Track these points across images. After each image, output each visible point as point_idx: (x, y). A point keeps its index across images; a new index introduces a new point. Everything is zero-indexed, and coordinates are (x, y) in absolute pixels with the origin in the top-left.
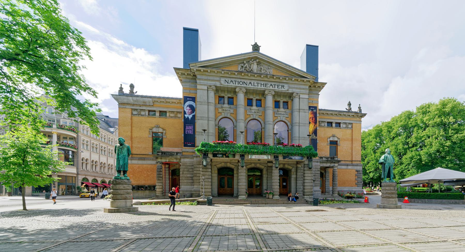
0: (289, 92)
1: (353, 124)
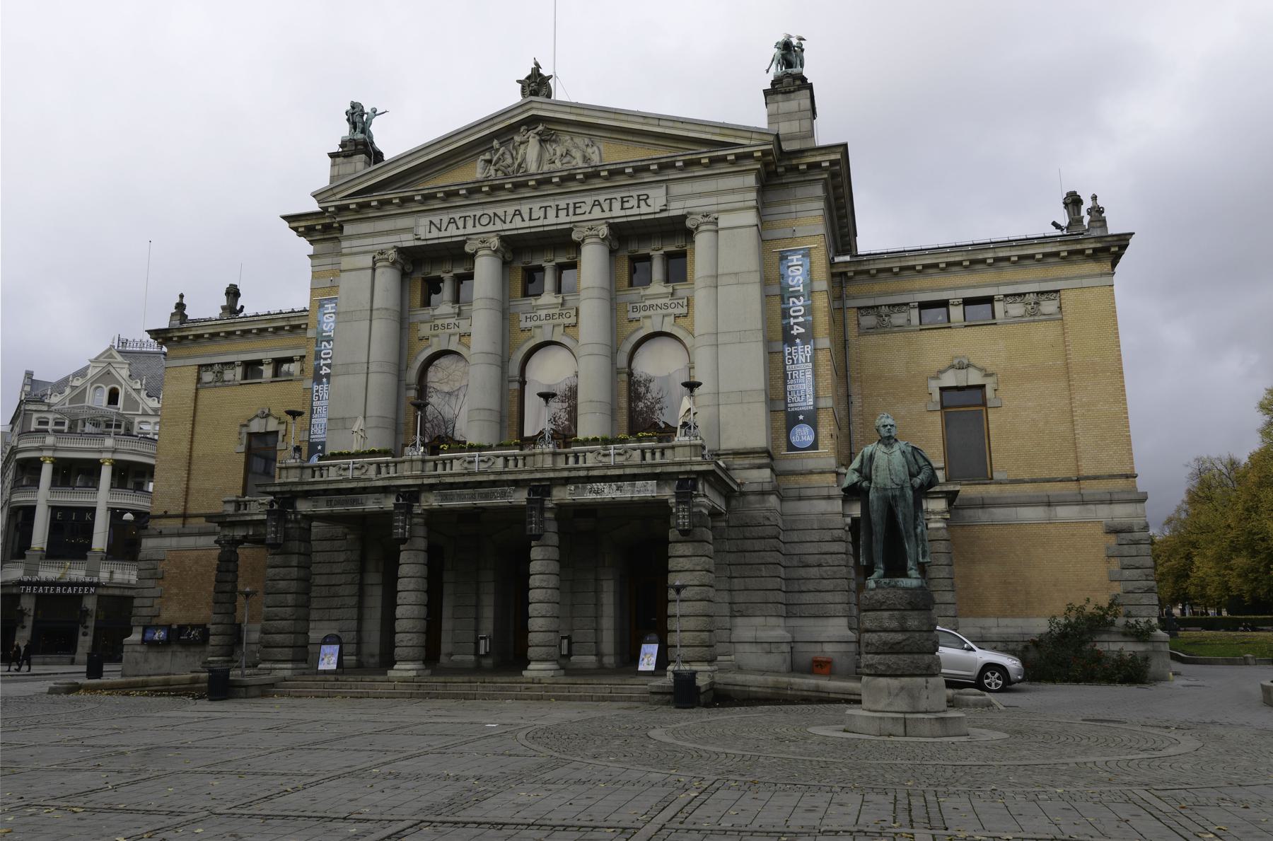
0: (672, 213)
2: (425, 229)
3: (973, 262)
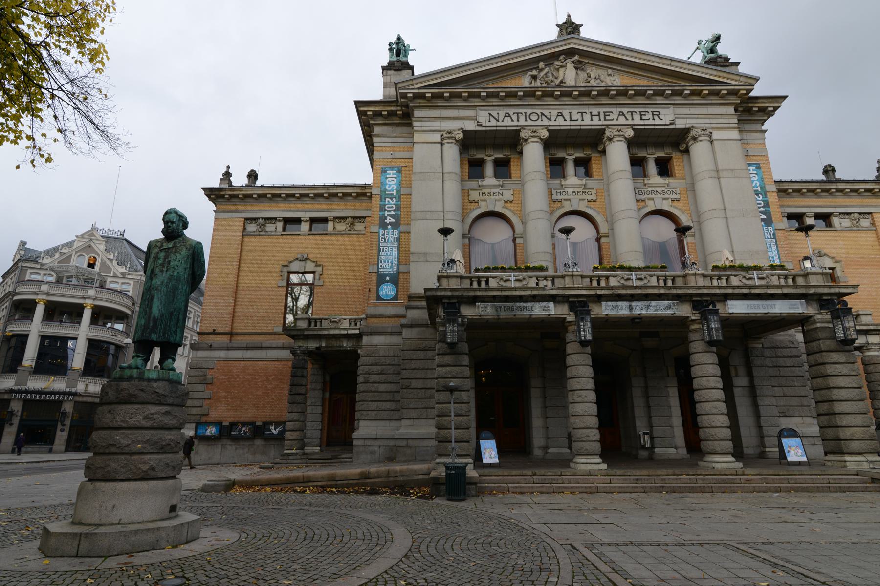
0: (678, 126)
1: (875, 216)
2: (486, 118)
3: (823, 191)
